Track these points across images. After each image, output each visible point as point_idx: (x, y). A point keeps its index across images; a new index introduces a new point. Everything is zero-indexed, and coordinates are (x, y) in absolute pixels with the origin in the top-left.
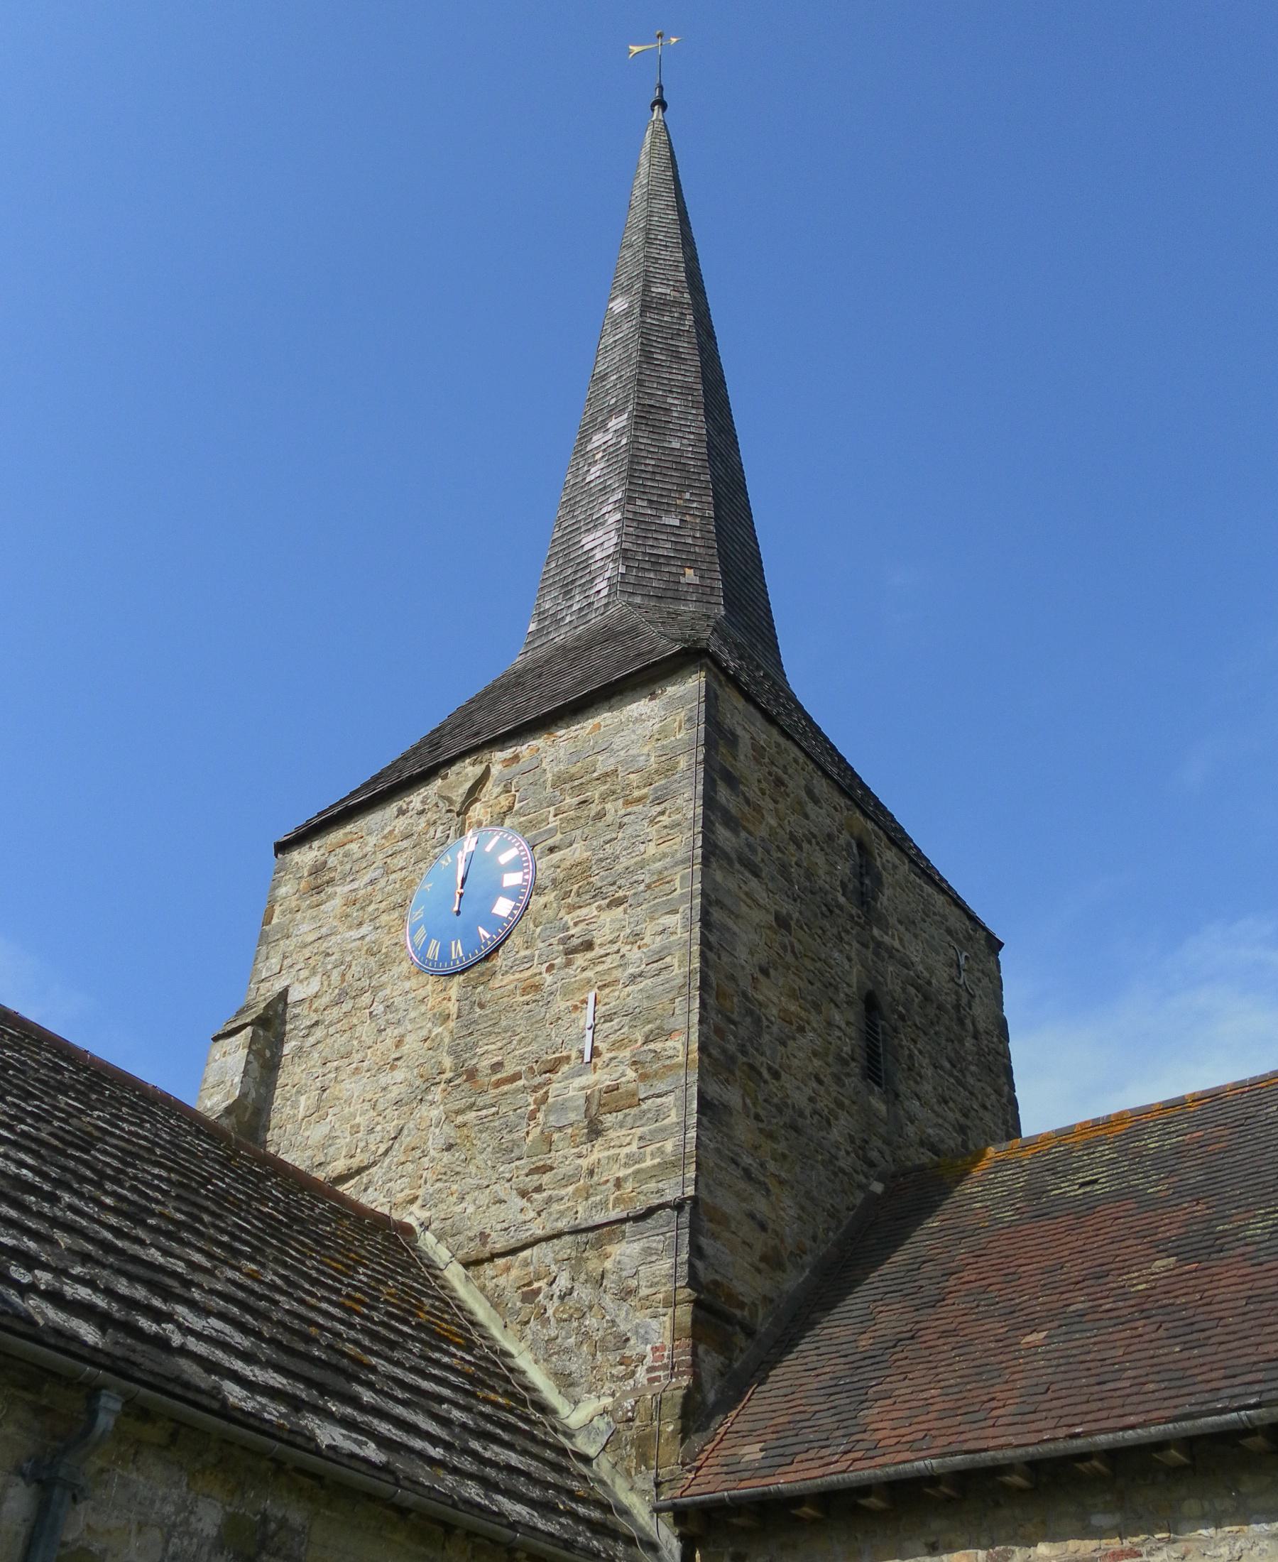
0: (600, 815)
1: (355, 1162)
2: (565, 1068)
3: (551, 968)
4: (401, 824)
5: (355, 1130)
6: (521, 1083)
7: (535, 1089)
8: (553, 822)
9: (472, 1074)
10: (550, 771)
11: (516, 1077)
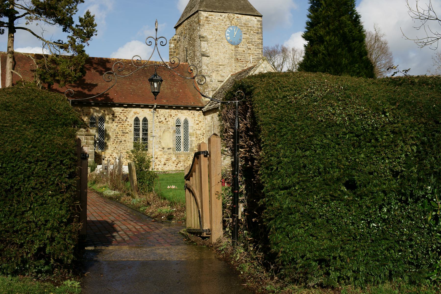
0: (250, 32)
1: (223, 64)
2: (248, 63)
4: (221, 18)
5: (222, 60)
8: (244, 30)
9: (237, 59)
10: (243, 22)
11: (243, 62)
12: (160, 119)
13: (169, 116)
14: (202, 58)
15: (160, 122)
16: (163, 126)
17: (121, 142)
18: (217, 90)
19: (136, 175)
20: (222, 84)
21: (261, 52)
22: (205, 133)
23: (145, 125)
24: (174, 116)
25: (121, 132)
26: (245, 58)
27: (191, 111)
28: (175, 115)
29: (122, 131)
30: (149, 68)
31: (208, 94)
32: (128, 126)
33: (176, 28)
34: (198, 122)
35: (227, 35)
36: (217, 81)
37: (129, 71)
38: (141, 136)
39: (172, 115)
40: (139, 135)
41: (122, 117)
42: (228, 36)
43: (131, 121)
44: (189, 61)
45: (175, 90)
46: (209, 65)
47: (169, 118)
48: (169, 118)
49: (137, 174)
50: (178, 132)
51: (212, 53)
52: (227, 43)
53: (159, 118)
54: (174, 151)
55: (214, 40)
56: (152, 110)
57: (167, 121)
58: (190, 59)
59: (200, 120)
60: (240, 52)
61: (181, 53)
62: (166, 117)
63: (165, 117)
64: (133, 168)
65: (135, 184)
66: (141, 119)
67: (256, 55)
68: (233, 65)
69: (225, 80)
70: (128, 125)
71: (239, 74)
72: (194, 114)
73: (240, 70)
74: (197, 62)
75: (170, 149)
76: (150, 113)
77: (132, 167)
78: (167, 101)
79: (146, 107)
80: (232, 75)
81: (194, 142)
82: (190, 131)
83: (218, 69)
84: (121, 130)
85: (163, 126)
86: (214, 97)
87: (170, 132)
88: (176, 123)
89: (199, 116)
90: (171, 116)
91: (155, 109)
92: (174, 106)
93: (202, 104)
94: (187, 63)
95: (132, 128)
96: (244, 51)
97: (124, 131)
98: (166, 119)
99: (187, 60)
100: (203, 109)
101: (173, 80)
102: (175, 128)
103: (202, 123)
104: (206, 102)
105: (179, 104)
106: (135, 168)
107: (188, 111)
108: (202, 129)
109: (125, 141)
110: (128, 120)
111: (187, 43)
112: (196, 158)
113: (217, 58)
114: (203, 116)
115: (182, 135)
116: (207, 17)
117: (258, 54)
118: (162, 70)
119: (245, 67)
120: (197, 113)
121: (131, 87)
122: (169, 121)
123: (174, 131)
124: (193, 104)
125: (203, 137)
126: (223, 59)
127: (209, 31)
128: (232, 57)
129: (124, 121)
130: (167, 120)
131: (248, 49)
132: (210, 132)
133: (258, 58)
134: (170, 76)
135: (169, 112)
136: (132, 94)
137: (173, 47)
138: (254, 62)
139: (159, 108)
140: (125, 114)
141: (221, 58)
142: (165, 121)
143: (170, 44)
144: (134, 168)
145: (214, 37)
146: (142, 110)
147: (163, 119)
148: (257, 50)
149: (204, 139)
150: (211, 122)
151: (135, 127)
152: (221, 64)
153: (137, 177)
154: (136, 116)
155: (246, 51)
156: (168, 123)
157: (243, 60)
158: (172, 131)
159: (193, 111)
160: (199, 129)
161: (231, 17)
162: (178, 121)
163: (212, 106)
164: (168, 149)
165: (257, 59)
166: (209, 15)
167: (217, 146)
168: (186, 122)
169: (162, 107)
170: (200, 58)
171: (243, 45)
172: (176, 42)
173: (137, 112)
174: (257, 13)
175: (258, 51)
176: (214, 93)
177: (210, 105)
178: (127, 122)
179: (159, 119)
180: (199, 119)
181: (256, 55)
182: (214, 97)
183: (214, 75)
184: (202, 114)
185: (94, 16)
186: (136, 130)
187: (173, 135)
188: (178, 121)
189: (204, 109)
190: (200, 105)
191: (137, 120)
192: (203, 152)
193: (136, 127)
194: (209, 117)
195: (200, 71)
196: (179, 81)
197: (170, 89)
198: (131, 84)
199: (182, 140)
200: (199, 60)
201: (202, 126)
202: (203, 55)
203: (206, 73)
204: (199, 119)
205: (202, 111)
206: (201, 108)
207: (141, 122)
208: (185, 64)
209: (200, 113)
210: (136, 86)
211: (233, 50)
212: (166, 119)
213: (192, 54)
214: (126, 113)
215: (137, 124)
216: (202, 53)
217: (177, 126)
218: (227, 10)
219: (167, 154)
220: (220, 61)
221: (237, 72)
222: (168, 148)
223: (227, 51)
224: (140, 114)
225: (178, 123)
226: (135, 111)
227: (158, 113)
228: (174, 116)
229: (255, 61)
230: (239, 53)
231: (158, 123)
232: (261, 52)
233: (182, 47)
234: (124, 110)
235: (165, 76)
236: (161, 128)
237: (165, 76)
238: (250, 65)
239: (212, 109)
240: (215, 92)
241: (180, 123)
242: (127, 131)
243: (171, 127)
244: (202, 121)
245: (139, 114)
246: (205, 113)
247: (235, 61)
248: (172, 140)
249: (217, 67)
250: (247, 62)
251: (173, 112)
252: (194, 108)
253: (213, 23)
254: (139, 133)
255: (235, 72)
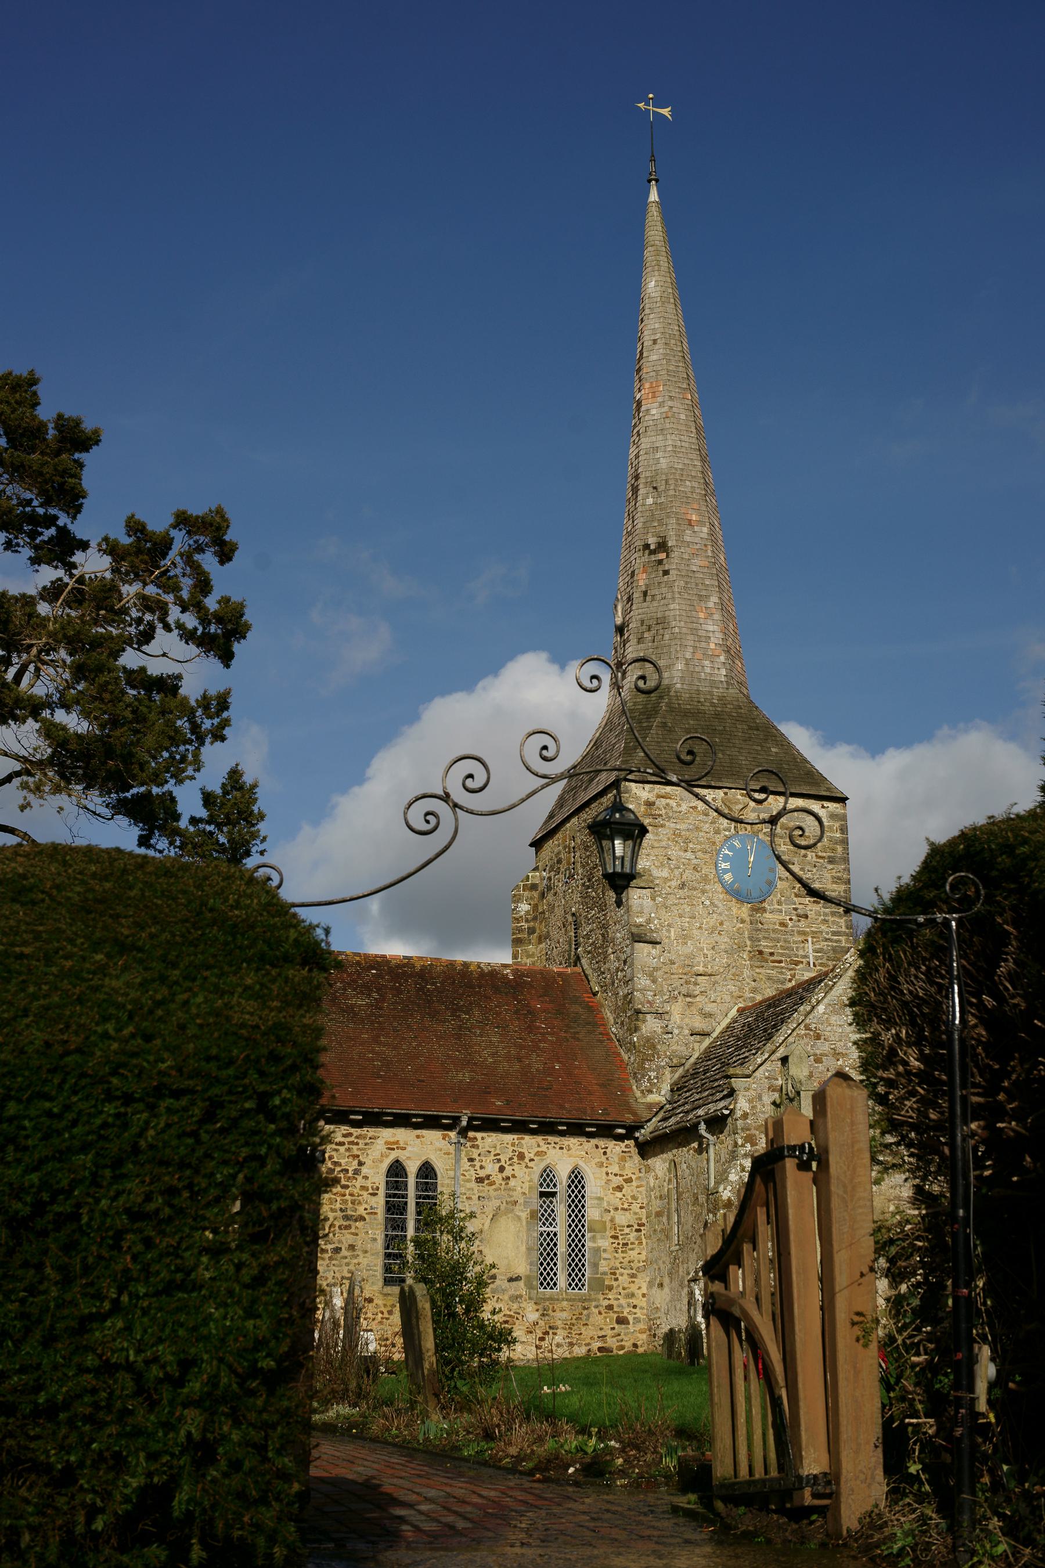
1: (709, 971)
2: (801, 966)
3: (791, 919)
5: (706, 956)
6: (783, 965)
7: (791, 970)
9: (761, 952)
11: (780, 962)
12: (482, 1167)
13: (515, 1159)
14: (633, 949)
15: (480, 1180)
16: (492, 1193)
17: (337, 1250)
18: (687, 1066)
19: (431, 1331)
20: (707, 1042)
21: (844, 929)
22: (644, 1221)
23: (426, 1190)
24: (532, 1156)
25: (339, 1214)
26: (787, 948)
27: (594, 1141)
28: (538, 1154)
29: (341, 1209)
30: (442, 983)
31: (657, 1078)
32: (365, 1193)
33: (537, 844)
34: (618, 1181)
35: (724, 865)
36: (687, 1032)
37: (369, 996)
38: (411, 1232)
39: (526, 1154)
40: (404, 1229)
41: (343, 1161)
42: (725, 871)
43: (376, 1175)
44: (583, 961)
45: (536, 1063)
46: (659, 973)
47: (516, 1167)
48: (516, 1167)
49: (435, 1330)
50: (548, 1217)
51: (669, 931)
52: (721, 896)
53: (478, 1164)
54: (530, 1286)
55: (674, 883)
56: (453, 1134)
57: (508, 1178)
58: (589, 952)
59: (628, 1173)
60: (771, 926)
61: (555, 934)
62: (503, 1163)
63: (499, 1161)
64: (420, 1305)
65: (426, 1365)
66: (412, 1168)
67: (826, 940)
68: (746, 973)
69: (719, 1030)
70: (364, 1188)
71: (769, 1006)
72: (605, 1153)
73: (770, 992)
74: (617, 964)
75: (518, 1279)
76: (444, 1144)
77: (419, 1298)
78: (508, 1102)
79: (432, 1122)
80: (741, 1011)
81: (604, 1255)
82: (592, 1213)
83: (691, 987)
84: (338, 1206)
85: (492, 1193)
86: (678, 1089)
87: (519, 1218)
88: (541, 1185)
89: (623, 1159)
90: (521, 1156)
91: (463, 1133)
92: (533, 1123)
93: (635, 1114)
94: (578, 969)
95: (379, 1202)
96: (783, 924)
97: (349, 1213)
98: (502, 1169)
99: (578, 959)
100: (637, 1135)
101: (529, 1026)
102: (536, 1202)
103: (634, 1183)
104: (650, 1106)
105: (552, 1113)
106: (428, 1306)
107: (584, 1139)
108: (635, 1207)
109: (352, 1247)
110: (365, 1170)
111: (577, 897)
112: (758, 1180)
113: (690, 948)
114: (637, 1158)
115: (561, 1228)
116: (650, 804)
117: (834, 933)
118: (490, 992)
119: (790, 980)
120: (615, 1148)
121: (377, 1053)
122: (514, 1176)
123: (533, 1215)
124: (600, 1114)
125: (639, 1238)
126: (709, 953)
127: (656, 851)
128: (741, 947)
129: (350, 1174)
130: (504, 1175)
131: (798, 916)
132: (664, 1219)
133: (834, 949)
134: (516, 1012)
135: (513, 1145)
136: (380, 1077)
137: (527, 912)
138: (821, 965)
139: (477, 1129)
140: (355, 1147)
141: (702, 949)
142: (500, 1176)
143: (514, 902)
144: (425, 1306)
145: (677, 872)
146: (418, 1137)
147: (491, 1169)
148: (831, 919)
149: (641, 1243)
150: (670, 1180)
151: (388, 1196)
152: (701, 969)
153: (435, 1339)
154: (393, 1156)
155: (790, 924)
156: (512, 1183)
157: (782, 955)
158: (524, 1215)
159: (602, 1142)
160: (626, 1206)
161: (737, 802)
162: (548, 1175)
163: (672, 1121)
164: (511, 1280)
165: (831, 954)
166: (659, 796)
167: (853, 1123)
168: (577, 1179)
169: (491, 1125)
170: (628, 950)
171: (779, 903)
172: (536, 894)
173: (397, 1142)
174: (828, 789)
175: (834, 922)
176: (677, 1075)
177: (664, 1119)
178: (360, 1178)
179: (477, 1167)
180: (622, 1168)
181: (826, 940)
182: (678, 1089)
183: (676, 1010)
184: (634, 1150)
185: (254, 786)
186: (395, 1208)
187: (528, 1230)
188: (548, 1175)
189: (643, 1134)
190: (629, 1118)
191: (396, 1170)
192: (793, 1148)
193: (395, 1196)
194: (659, 1164)
195: (625, 996)
196: (548, 1033)
197: (519, 1059)
198: (376, 1040)
199: (562, 1248)
200: (623, 957)
201: (634, 1197)
202: (638, 938)
203: (649, 1002)
204: (622, 1168)
205: (636, 1139)
206: (631, 1131)
207: (412, 1181)
208: (569, 970)
209: (626, 1146)
210: (395, 1048)
211: (743, 921)
212: (502, 1169)
213: (596, 937)
214: (357, 1144)
215: (396, 1185)
216: (634, 930)
217: (542, 1194)
218: (720, 779)
219: (506, 1297)
220: (698, 959)
221: (759, 998)
222: (509, 1275)
223: (721, 924)
224: (409, 1148)
225: (548, 1185)
226: (392, 1140)
227: (473, 1146)
228: (532, 1160)
229: (824, 961)
230: (767, 931)
231: (473, 1185)
232: (844, 929)
233: (559, 912)
234: (351, 1135)
235: (498, 1014)
236: (486, 1202)
237: (498, 1014)
238: (808, 975)
239: (673, 1132)
240: (680, 1071)
241: (555, 1186)
242: (361, 1210)
243: (521, 1201)
244: (634, 1177)
245: (404, 1149)
246: (646, 1149)
247: (751, 959)
248: (523, 1248)
249: (687, 982)
250: (797, 963)
251: (529, 1143)
252: (605, 1131)
253: (673, 825)
254: (404, 1221)
255: (753, 999)
